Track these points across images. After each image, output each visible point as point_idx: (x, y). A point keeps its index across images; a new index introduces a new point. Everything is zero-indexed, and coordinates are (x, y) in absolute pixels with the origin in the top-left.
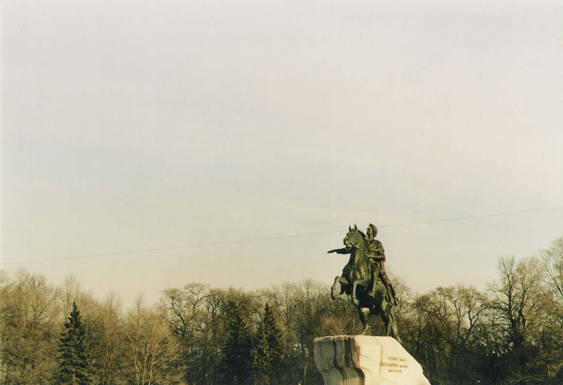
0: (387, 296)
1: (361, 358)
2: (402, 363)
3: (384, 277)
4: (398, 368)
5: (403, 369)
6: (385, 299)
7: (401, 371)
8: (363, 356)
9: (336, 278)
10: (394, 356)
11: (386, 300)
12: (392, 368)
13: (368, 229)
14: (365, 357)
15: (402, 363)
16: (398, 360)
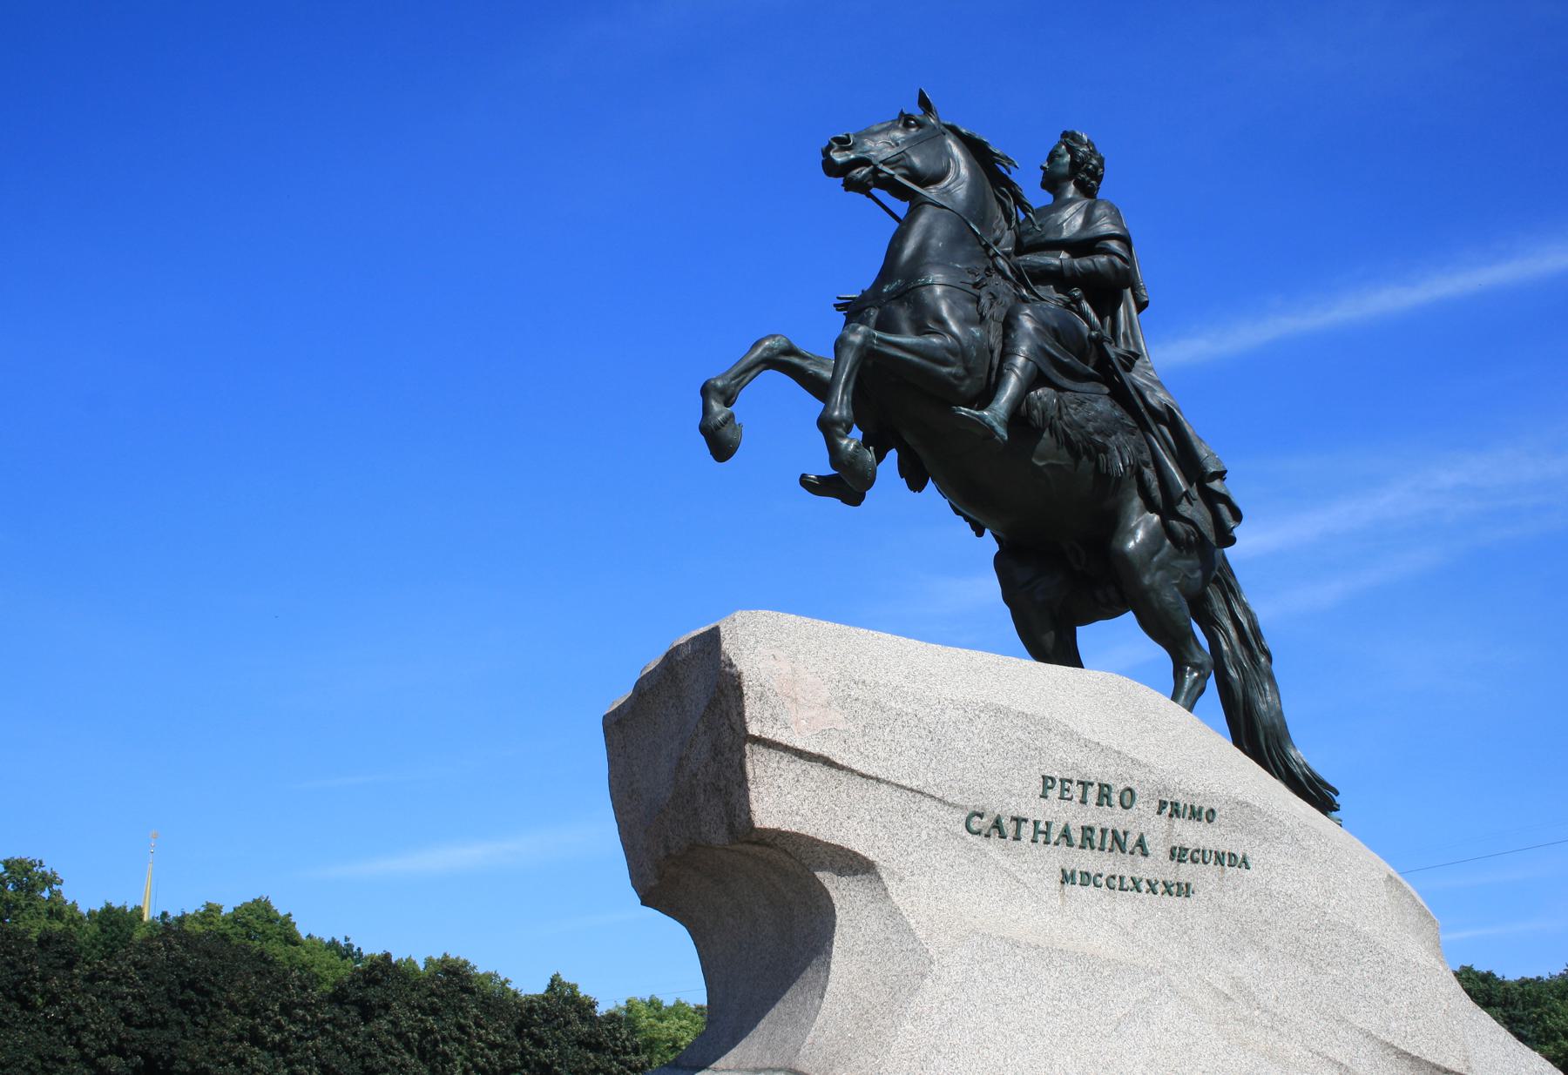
0: (1149, 474)
1: (758, 765)
2: (1190, 834)
3: (1137, 377)
4: (1156, 866)
5: (1202, 876)
6: (1137, 502)
7: (1185, 890)
8: (758, 741)
9: (757, 344)
10: (1095, 771)
11: (1150, 506)
12: (1088, 861)
13: (1053, 157)
14: (800, 754)
15: (1190, 834)
16: (1145, 806)
